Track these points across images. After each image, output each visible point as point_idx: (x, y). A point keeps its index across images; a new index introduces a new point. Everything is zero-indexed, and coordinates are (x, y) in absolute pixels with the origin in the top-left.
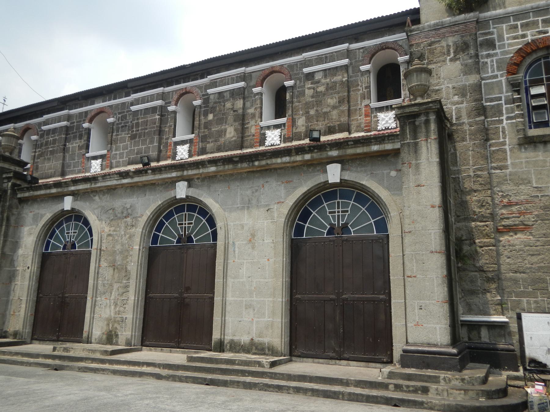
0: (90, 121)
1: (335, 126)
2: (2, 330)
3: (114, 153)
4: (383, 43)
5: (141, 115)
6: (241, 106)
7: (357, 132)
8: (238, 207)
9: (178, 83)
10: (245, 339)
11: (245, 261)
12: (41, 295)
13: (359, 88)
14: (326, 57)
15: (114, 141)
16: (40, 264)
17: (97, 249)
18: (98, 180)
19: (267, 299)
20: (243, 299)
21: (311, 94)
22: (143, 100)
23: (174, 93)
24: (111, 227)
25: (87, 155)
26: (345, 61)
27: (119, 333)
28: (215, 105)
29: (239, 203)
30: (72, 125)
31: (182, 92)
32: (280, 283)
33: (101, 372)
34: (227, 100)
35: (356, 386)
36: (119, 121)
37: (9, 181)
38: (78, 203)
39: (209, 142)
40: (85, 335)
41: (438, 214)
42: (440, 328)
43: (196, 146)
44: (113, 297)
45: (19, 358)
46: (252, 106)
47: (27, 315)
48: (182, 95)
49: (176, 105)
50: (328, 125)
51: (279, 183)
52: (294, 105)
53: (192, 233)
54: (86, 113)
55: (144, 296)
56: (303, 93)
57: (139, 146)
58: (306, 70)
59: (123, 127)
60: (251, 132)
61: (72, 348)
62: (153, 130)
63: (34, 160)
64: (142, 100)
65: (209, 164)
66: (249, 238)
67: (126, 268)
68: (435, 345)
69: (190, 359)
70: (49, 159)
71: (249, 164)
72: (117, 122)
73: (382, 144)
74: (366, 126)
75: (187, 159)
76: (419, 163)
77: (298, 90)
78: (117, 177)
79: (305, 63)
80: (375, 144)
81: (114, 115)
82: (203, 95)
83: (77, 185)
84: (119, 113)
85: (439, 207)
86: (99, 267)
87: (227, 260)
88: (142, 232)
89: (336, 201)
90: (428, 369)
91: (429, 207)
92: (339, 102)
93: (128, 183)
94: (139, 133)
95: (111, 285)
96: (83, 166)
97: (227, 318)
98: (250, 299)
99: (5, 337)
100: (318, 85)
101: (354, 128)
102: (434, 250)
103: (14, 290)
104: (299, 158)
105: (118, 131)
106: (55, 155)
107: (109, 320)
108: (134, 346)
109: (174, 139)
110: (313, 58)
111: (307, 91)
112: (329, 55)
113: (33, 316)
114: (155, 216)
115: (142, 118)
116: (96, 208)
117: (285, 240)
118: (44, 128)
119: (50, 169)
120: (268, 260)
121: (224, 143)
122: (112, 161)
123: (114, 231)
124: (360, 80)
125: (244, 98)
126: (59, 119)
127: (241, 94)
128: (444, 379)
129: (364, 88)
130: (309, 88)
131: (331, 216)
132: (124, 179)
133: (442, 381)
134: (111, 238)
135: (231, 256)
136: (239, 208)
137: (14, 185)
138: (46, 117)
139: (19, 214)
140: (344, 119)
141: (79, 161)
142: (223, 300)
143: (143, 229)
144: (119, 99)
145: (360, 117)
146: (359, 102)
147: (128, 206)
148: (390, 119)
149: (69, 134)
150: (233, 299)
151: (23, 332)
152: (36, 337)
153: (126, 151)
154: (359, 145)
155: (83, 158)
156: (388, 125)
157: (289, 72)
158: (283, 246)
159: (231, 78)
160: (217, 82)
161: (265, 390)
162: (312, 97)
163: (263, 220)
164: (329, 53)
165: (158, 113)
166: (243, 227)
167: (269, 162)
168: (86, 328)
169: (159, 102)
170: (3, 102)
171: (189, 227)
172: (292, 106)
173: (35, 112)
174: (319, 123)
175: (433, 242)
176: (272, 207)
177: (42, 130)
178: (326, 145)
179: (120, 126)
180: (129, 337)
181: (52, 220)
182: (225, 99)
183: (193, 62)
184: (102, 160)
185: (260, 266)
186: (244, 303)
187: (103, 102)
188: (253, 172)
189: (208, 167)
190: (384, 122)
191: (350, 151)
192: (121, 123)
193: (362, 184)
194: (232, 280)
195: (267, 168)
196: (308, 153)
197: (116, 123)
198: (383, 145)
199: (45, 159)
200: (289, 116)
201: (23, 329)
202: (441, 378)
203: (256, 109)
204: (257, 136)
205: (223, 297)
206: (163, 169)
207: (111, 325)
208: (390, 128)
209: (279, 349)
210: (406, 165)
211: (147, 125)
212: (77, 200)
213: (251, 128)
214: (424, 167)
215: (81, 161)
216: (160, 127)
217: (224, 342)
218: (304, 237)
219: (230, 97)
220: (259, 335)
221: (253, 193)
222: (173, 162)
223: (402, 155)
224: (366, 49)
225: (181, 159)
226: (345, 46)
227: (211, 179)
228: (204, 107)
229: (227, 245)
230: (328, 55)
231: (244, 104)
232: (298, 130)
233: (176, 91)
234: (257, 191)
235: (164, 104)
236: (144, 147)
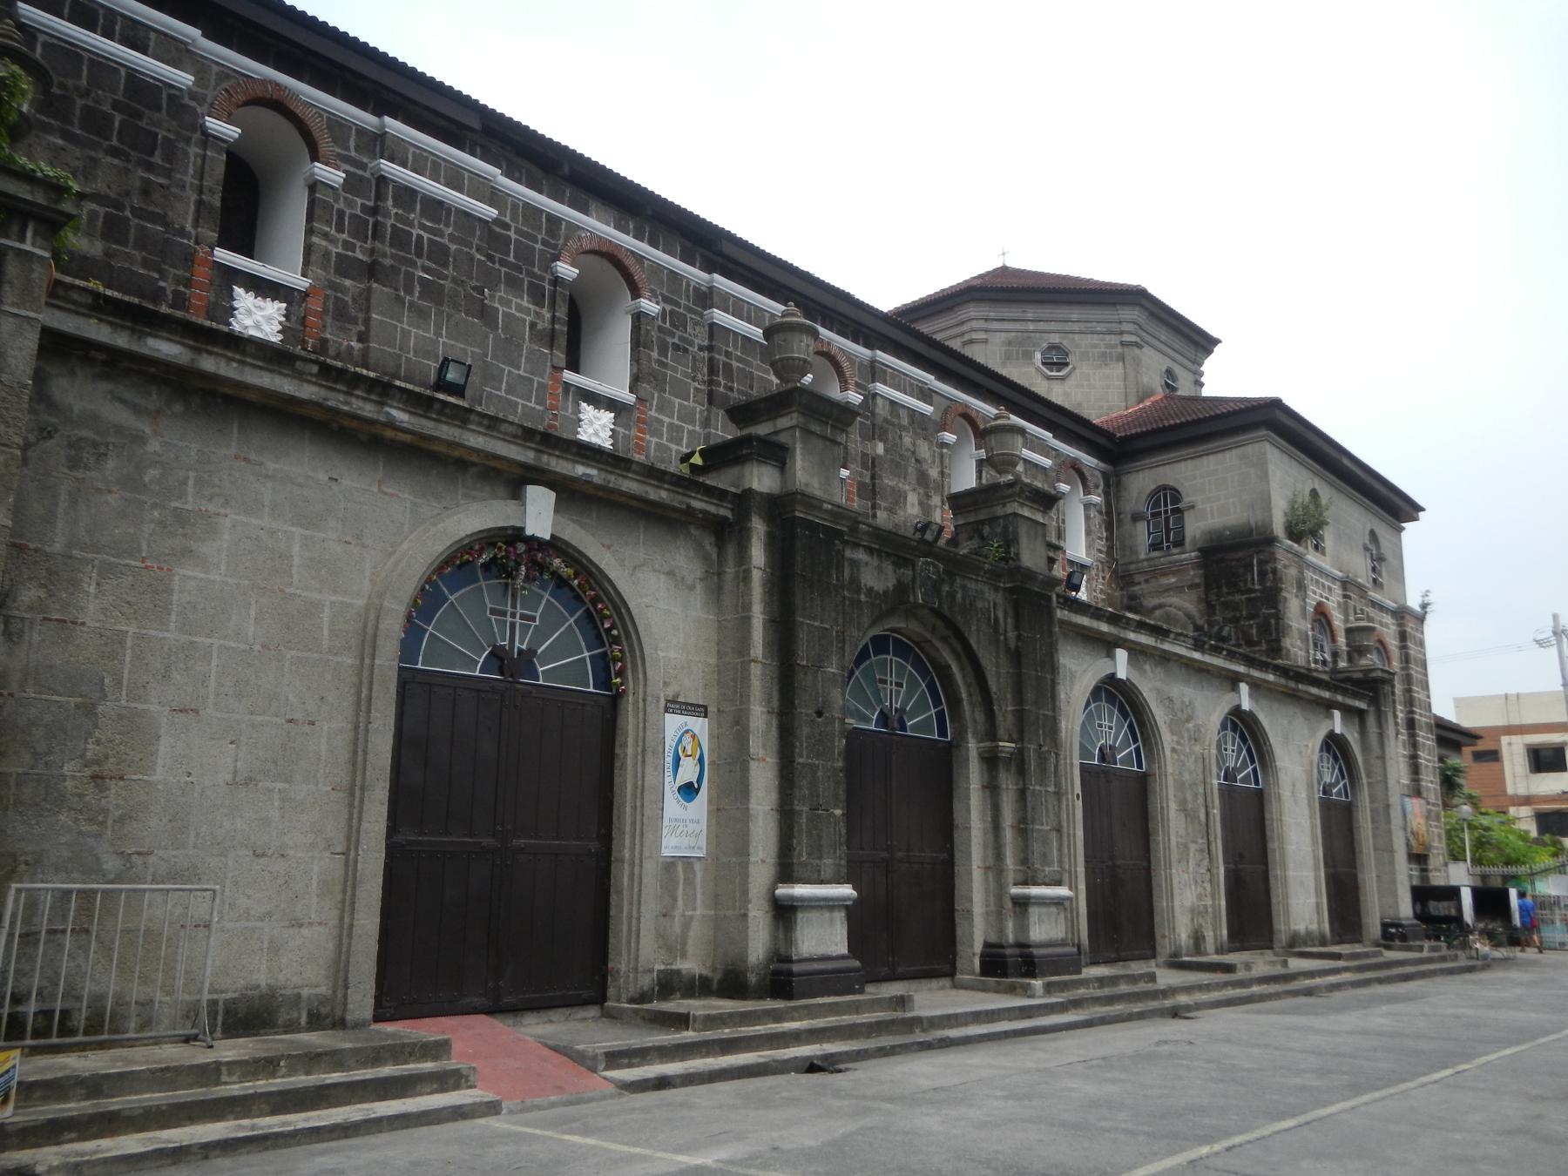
18: (1168, 637)
30: (497, 229)
59: (676, 347)
70: (422, 314)
72: (660, 323)
95: (1186, 847)
96: (553, 407)
106: (446, 308)
118: (389, 168)
121: (905, 522)
138: (394, 126)
141: (531, 381)
153: (690, 427)
155: (553, 378)
173: (308, 51)
215: (542, 386)
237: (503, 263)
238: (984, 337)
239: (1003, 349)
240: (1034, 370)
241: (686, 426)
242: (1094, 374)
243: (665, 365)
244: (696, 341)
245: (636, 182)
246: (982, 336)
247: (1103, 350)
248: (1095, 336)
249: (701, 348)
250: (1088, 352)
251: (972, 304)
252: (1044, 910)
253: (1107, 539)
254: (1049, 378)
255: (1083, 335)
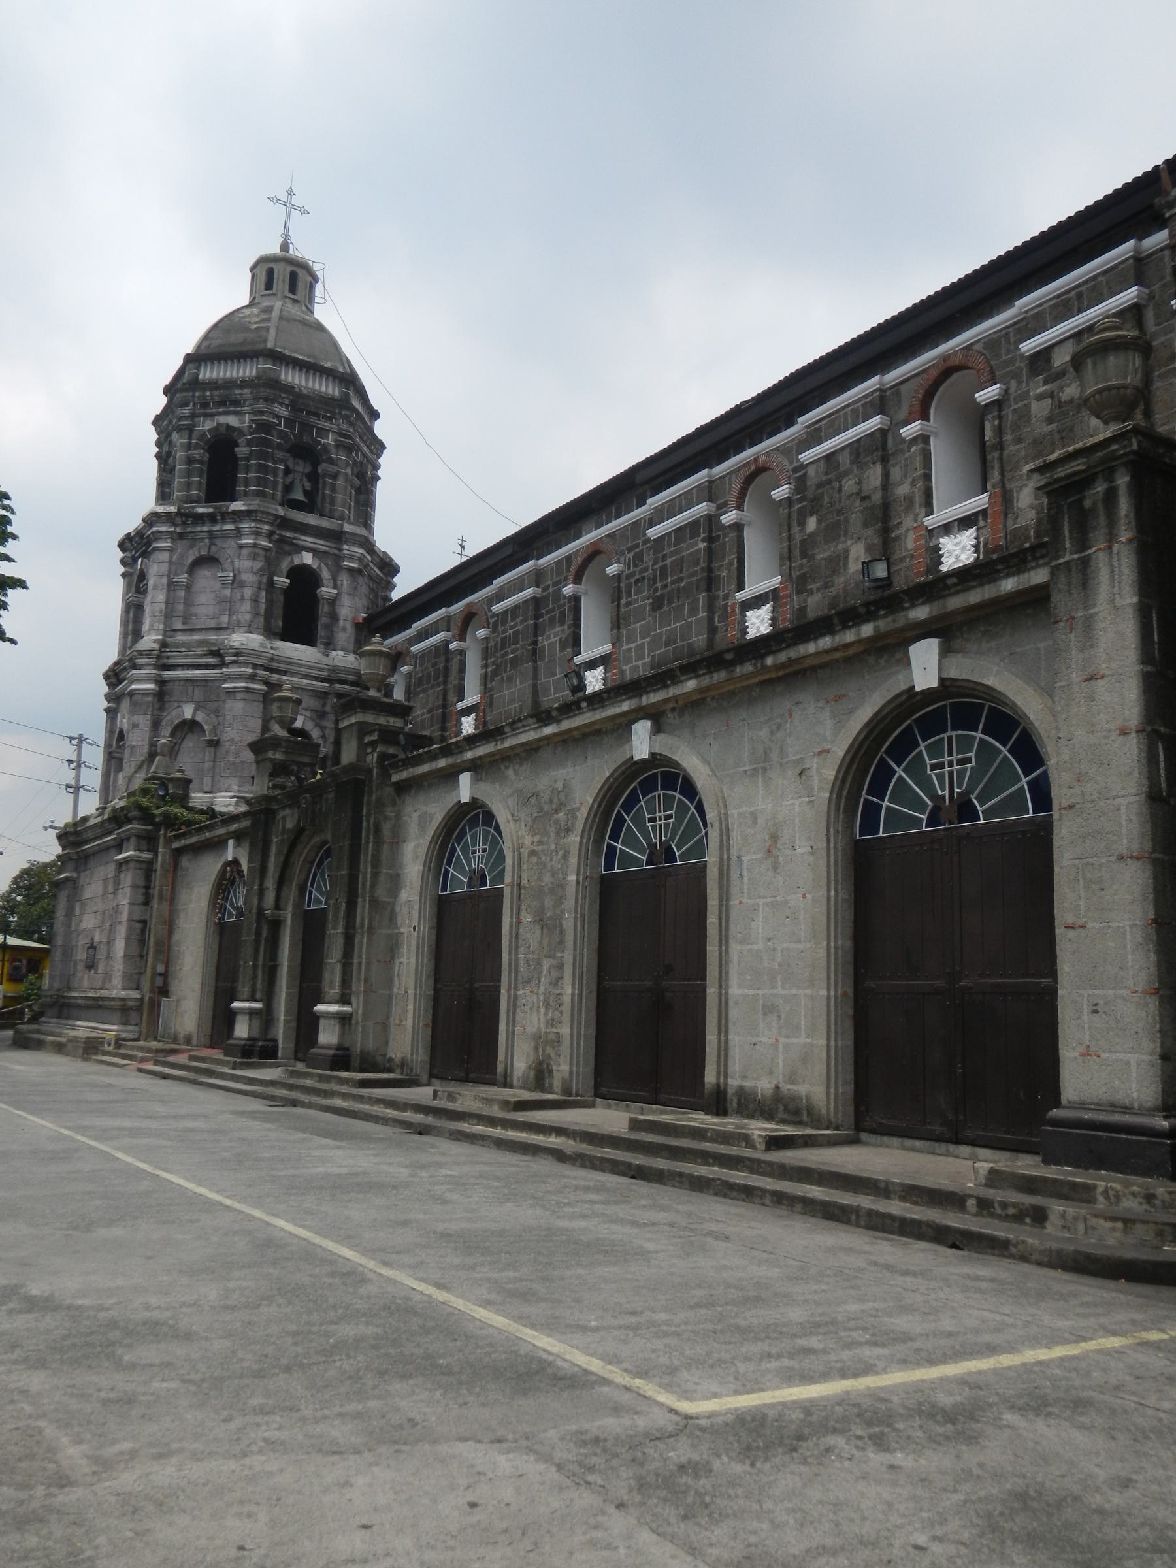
0: (577, 580)
2: (385, 1055)
3: (625, 647)
6: (878, 483)
8: (746, 771)
9: (739, 449)
10: (763, 1085)
11: (761, 902)
12: (439, 986)
14: (1080, 296)
16: (435, 920)
17: (512, 885)
18: (505, 733)
19: (801, 992)
20: (760, 992)
21: (1046, 413)
24: (535, 834)
25: (578, 660)
27: (554, 1068)
28: (820, 491)
29: (747, 760)
31: (748, 472)
32: (822, 953)
33: (480, 1142)
34: (847, 473)
35: (903, 1199)
36: (629, 569)
37: (374, 750)
38: (483, 786)
39: (811, 592)
40: (500, 1068)
41: (1136, 751)
42: (1138, 1064)
43: (786, 604)
44: (542, 989)
45: (377, 1109)
46: (905, 476)
47: (419, 1025)
48: (749, 480)
49: (739, 507)
51: (820, 704)
52: (1006, 453)
53: (672, 839)
54: (569, 559)
55: (594, 987)
56: (1024, 415)
58: (1028, 346)
59: (637, 581)
60: (906, 549)
61: (459, 1094)
62: (694, 579)
63: (485, 685)
64: (669, 506)
65: (682, 674)
66: (767, 844)
67: (561, 925)
68: (1126, 1109)
69: (635, 1125)
71: (755, 665)
72: (627, 572)
73: (1024, 572)
76: (1092, 616)
77: (1015, 407)
78: (534, 724)
79: (1027, 324)
80: (1008, 576)
82: (795, 470)
83: (474, 748)
84: (630, 550)
85: (1138, 732)
86: (519, 923)
87: (728, 899)
88: (581, 843)
89: (945, 736)
90: (1100, 1169)
91: (1114, 735)
93: (555, 735)
94: (669, 592)
95: (539, 964)
97: (730, 1037)
98: (772, 991)
99: (390, 1071)
100: (1063, 381)
102: (1125, 852)
103: (398, 975)
104: (849, 636)
105: (629, 594)
107: (537, 1038)
108: (577, 1095)
109: (741, 596)
110: (1045, 306)
111: (1035, 407)
112: (1086, 287)
113: (430, 1029)
114: (604, 804)
115: (673, 554)
116: (511, 795)
117: (832, 845)
118: (497, 608)
119: (513, 701)
120: (804, 896)
122: (624, 668)
123: (540, 843)
125: (885, 460)
126: (518, 585)
127: (877, 449)
128: (1106, 1192)
130: (1040, 398)
131: (936, 775)
132: (546, 725)
133: (1101, 1199)
134: (535, 860)
135: (734, 890)
136: (748, 773)
137: (383, 757)
138: (498, 582)
139: (398, 816)
142: (720, 994)
143: (582, 837)
147: (559, 786)
149: (542, 616)
150: (740, 992)
151: (412, 1060)
152: (435, 1071)
153: (648, 639)
154: (972, 584)
157: (988, 361)
158: (828, 862)
159: (852, 409)
160: (819, 429)
161: (725, 1196)
162: (1050, 420)
163: (792, 798)
165: (702, 535)
166: (754, 816)
167: (793, 653)
168: (501, 1056)
169: (701, 509)
170: (459, 550)
171: (667, 825)
172: (1001, 459)
175: (1124, 831)
176: (808, 766)
177: (494, 615)
178: (901, 595)
179: (633, 580)
180: (567, 1075)
181: (446, 824)
182: (842, 469)
183: (760, 392)
184: (605, 669)
185: (788, 912)
186: (761, 1001)
187: (596, 529)
188: (770, 682)
189: (682, 682)
191: (955, 602)
192: (633, 574)
193: (987, 686)
194: (739, 947)
195: (796, 668)
196: (868, 621)
198: (1026, 575)
199: (503, 679)
200: (994, 487)
201: (412, 1055)
202: (1100, 1190)
203: (913, 484)
204: (920, 556)
205: (720, 987)
206: (605, 696)
207: (540, 1049)
209: (824, 1111)
210: (1062, 624)
211: (681, 571)
212: (481, 780)
213: (906, 537)
214: (1103, 625)
216: (710, 570)
217: (725, 1092)
218: (881, 834)
219: (852, 462)
220: (790, 1078)
221: (772, 733)
223: (1056, 598)
227: (694, 706)
228: (800, 500)
229: (725, 863)
231: (886, 475)
232: (1021, 522)
234: (779, 727)
235: (714, 509)
236: (679, 624)
237: (547, 612)
245: (799, 368)
252: (327, 1021)
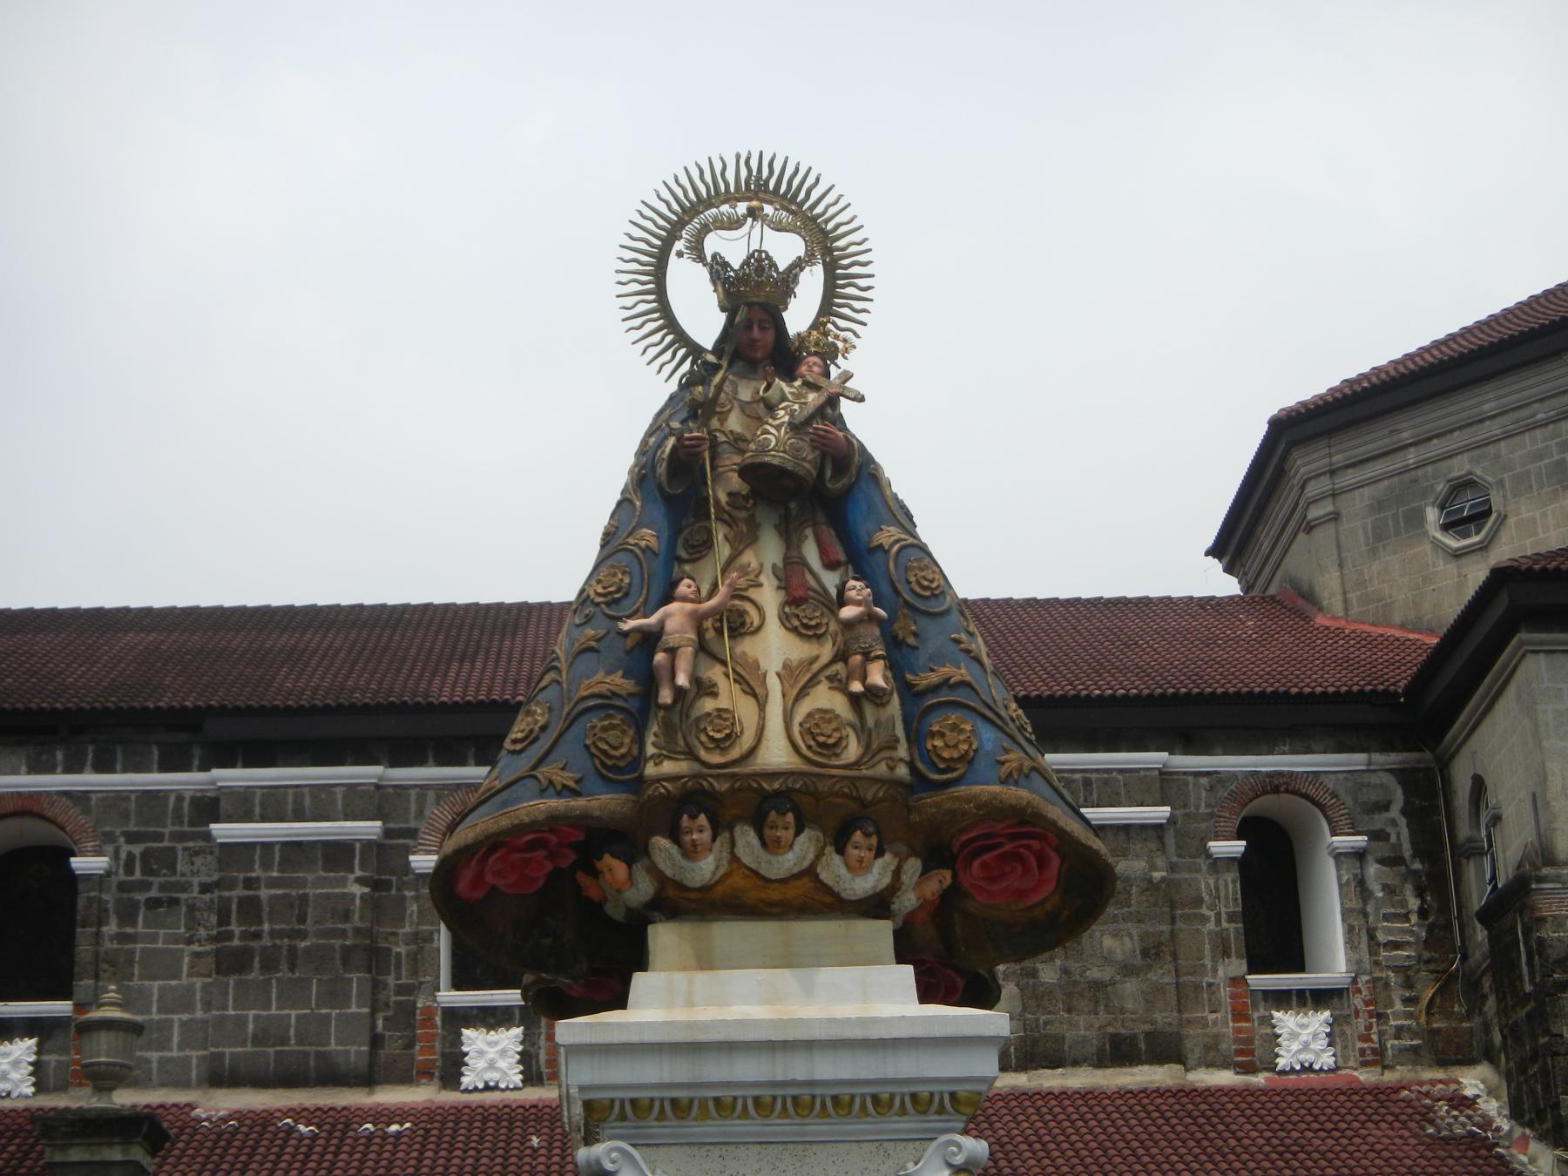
1: (1134, 1037)
4: (1280, 774)
5: (267, 865)
7: (1208, 1066)
13: (1205, 911)
15: (111, 963)
22: (274, 805)
23: (431, 795)
26: (1161, 813)
50: (1111, 1030)
57: (267, 1006)
59: (153, 904)
62: (337, 943)
72: (122, 876)
74: (1239, 1053)
75: (516, 1089)
81: (104, 841)
84: (132, 838)
92: (1145, 953)
101: (1197, 1050)
115: (273, 883)
124: (1208, 885)
129: (1224, 916)
140: (1164, 1018)
144: (125, 770)
145: (1213, 1016)
146: (1208, 962)
148: (1315, 1036)
153: (185, 1017)
156: (1307, 1057)
164: (1098, 771)
165: (358, 873)
174: (1075, 1017)
184: (39, 1045)
187: (33, 770)
190: (1295, 1046)
197: (114, 880)
208: (1317, 1067)
211: (302, 919)
222: (450, 1097)
224: (1220, 781)
225: (487, 1088)
226: (1154, 759)
230: (1093, 776)
233: (444, 791)
238: (1330, 508)
239: (1369, 521)
240: (1428, 547)
241: (176, 1017)
242: (1544, 515)
243: (132, 938)
244: (196, 881)
246: (1326, 508)
247: (1556, 458)
248: (1538, 433)
249: (205, 888)
250: (1528, 472)
251: (1295, 454)
253: (1423, 913)
254: (1458, 555)
255: (1517, 439)
